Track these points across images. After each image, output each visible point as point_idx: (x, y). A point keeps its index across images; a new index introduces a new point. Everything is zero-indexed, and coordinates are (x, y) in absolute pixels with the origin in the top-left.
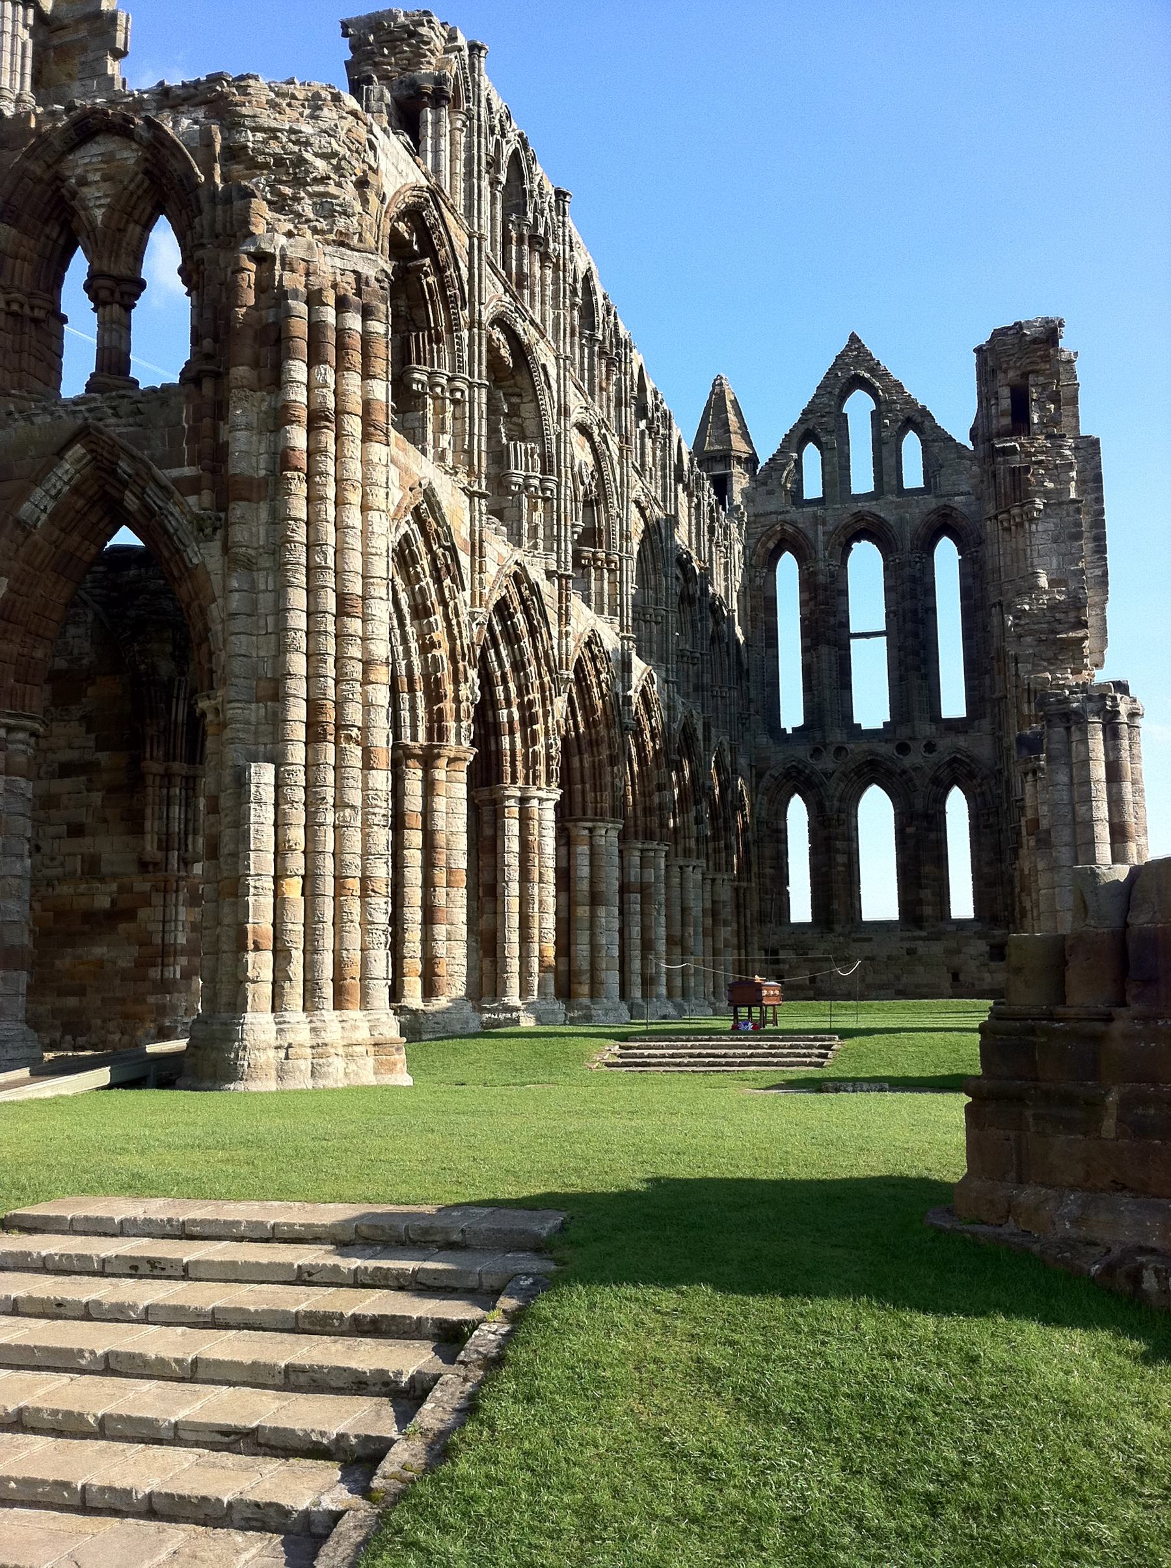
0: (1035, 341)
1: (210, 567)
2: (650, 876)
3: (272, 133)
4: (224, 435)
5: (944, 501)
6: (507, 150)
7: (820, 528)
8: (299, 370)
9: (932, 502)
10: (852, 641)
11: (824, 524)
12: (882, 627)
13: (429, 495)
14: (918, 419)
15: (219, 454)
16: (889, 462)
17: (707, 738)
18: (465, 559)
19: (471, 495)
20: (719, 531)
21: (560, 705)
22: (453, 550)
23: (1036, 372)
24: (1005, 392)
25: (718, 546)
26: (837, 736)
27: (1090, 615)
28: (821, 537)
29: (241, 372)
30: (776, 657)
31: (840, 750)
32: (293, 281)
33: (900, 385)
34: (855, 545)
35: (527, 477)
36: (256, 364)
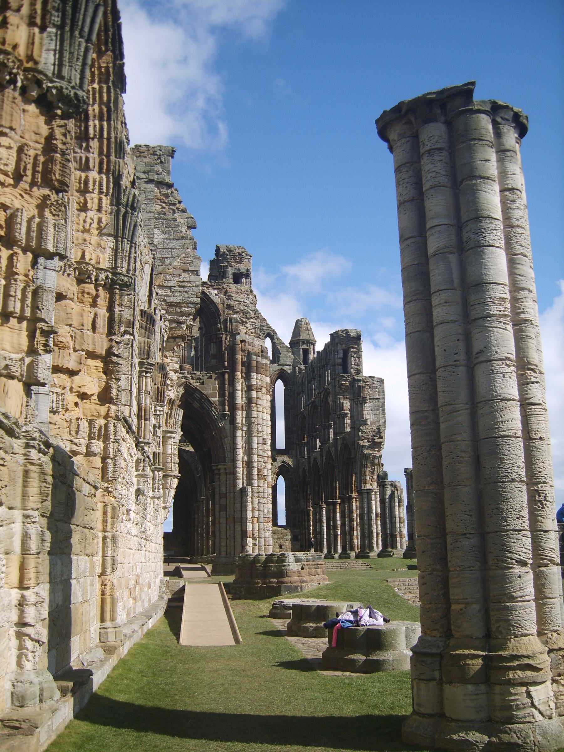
0: (354, 337)
1: (226, 428)
5: (280, 367)
8: (254, 375)
9: (276, 367)
23: (353, 348)
24: (341, 351)
27: (382, 434)
32: (250, 349)
33: (265, 320)
36: (242, 373)
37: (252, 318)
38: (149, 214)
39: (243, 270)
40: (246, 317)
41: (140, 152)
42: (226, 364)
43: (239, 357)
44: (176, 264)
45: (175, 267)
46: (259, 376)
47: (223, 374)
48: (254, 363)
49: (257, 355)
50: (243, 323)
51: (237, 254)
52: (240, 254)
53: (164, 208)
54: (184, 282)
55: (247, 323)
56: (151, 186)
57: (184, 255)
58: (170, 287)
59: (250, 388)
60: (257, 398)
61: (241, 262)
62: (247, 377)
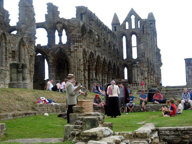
2: (105, 78)
4: (70, 48)
8: (76, 43)
10: (133, 48)
15: (70, 49)
16: (137, 24)
17: (112, 62)
18: (87, 53)
20: (114, 36)
21: (95, 63)
24: (142, 26)
26: (130, 60)
29: (72, 43)
30: (123, 50)
31: (131, 62)
34: (133, 35)
46: (78, 43)
50: (74, 30)
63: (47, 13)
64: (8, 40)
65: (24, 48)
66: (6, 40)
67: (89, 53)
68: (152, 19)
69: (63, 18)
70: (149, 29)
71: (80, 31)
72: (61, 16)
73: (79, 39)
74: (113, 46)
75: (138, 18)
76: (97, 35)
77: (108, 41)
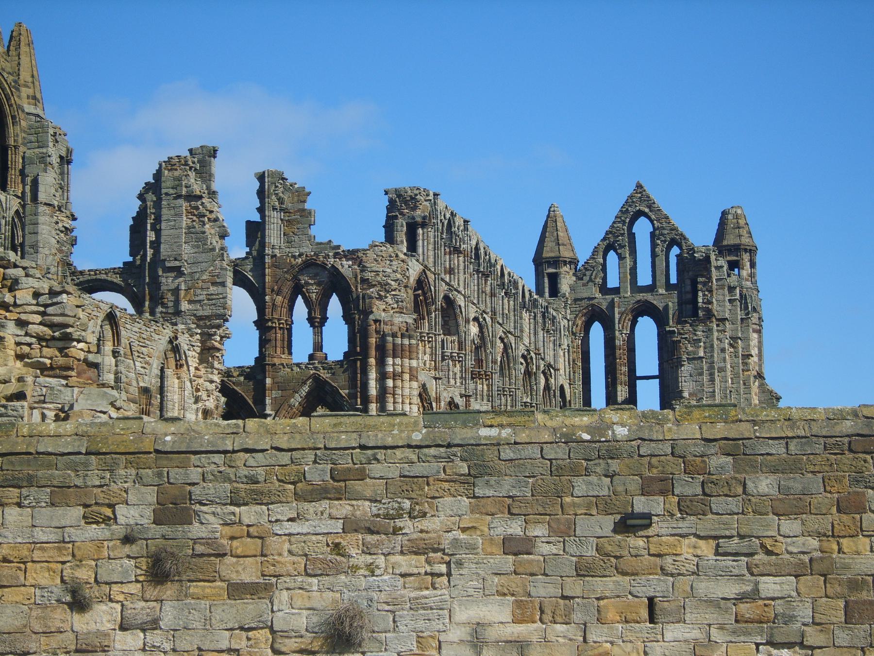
0: (700, 260)
3: (377, 273)
6: (446, 222)
7: (616, 310)
8: (390, 361)
11: (619, 307)
12: (657, 373)
13: (424, 386)
14: (678, 240)
18: (434, 404)
19: (436, 379)
20: (548, 325)
22: (431, 404)
23: (702, 276)
25: (548, 331)
28: (617, 316)
32: (387, 329)
33: (667, 218)
34: (640, 319)
35: (451, 353)
37: (395, 290)
38: (178, 231)
39: (419, 219)
40: (386, 290)
41: (172, 165)
42: (358, 349)
43: (373, 341)
44: (204, 277)
45: (203, 281)
46: (398, 361)
47: (355, 361)
48: (390, 346)
49: (394, 335)
50: (380, 298)
51: (409, 198)
52: (412, 198)
53: (194, 221)
54: (212, 294)
55: (386, 297)
56: (181, 201)
57: (212, 268)
58: (200, 301)
59: (383, 376)
60: (394, 387)
61: (415, 208)
62: (381, 363)
63: (256, 217)
64: (124, 341)
65: (178, 378)
66: (119, 340)
67: (442, 404)
68: (737, 241)
69: (330, 241)
70: (724, 295)
71: (409, 304)
72: (321, 232)
73: (406, 342)
74: (544, 372)
75: (667, 237)
76: (476, 319)
77: (522, 350)
